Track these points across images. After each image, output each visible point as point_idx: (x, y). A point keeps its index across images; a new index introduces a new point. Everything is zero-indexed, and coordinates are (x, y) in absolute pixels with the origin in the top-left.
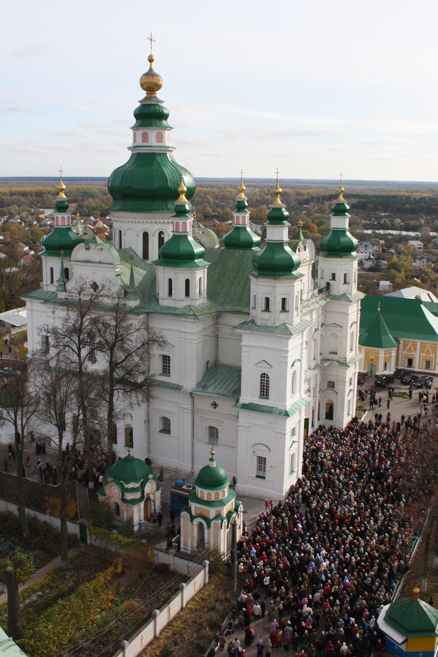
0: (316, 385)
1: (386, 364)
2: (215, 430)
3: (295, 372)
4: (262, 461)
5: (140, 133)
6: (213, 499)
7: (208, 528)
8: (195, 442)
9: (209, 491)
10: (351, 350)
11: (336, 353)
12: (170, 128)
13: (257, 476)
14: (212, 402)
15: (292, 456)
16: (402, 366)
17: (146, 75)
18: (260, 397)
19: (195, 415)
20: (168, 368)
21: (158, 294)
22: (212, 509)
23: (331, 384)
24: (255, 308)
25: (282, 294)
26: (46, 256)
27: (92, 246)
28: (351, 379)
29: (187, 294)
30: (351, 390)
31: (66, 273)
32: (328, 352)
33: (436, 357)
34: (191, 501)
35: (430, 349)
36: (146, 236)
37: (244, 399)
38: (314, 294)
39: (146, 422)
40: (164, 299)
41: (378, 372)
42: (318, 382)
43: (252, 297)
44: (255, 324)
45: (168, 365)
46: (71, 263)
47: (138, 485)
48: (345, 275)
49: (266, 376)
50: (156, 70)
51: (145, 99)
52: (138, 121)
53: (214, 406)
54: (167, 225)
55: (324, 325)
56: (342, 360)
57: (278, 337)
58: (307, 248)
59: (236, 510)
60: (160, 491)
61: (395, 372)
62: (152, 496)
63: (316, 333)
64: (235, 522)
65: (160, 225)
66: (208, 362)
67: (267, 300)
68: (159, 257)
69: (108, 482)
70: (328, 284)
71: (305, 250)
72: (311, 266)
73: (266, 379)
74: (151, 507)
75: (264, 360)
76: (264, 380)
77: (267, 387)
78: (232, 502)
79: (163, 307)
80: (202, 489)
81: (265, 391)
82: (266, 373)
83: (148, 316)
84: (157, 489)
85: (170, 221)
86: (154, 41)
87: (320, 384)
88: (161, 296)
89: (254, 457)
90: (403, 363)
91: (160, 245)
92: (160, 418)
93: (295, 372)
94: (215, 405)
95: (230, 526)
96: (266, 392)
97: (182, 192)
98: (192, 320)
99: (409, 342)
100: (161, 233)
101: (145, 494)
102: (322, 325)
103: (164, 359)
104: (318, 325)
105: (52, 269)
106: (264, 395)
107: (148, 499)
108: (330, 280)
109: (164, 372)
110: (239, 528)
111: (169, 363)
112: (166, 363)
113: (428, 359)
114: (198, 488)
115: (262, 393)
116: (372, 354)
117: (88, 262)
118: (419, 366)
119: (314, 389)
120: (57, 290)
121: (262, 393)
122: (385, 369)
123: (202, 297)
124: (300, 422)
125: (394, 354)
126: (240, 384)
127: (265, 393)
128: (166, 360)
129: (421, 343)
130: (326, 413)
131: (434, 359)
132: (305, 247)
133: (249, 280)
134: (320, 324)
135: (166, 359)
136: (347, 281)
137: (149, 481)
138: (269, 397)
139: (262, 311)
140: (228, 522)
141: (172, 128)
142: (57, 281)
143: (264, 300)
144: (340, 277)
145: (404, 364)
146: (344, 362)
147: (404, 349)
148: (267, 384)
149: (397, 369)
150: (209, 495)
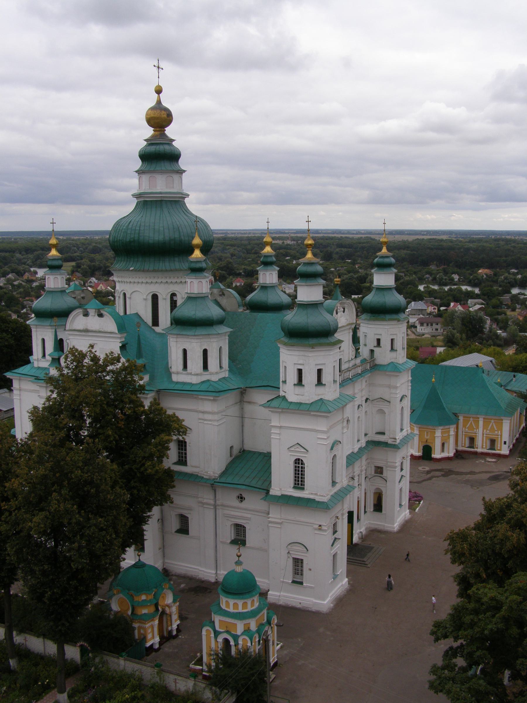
0: (361, 471)
1: (443, 445)
2: (242, 528)
3: (335, 456)
4: (298, 563)
5: (145, 177)
6: (240, 610)
7: (235, 645)
8: (218, 542)
9: (236, 601)
10: (402, 430)
11: (383, 433)
12: (181, 172)
13: (294, 582)
14: (238, 494)
16: (462, 446)
17: (152, 109)
18: (294, 488)
19: (217, 510)
20: (184, 455)
21: (171, 367)
22: (239, 622)
23: (379, 470)
24: (285, 382)
25: (316, 365)
26: (36, 325)
27: (92, 312)
28: (402, 463)
29: (205, 367)
30: (402, 476)
31: (59, 344)
32: (374, 433)
33: (501, 435)
34: (214, 614)
35: (494, 425)
36: (155, 298)
37: (275, 491)
38: (356, 365)
39: (160, 521)
40: (178, 373)
41: (434, 454)
42: (364, 468)
43: (282, 370)
44: (287, 400)
45: (184, 452)
46: (67, 333)
47: (151, 597)
48: (392, 340)
49: (300, 462)
50: (165, 104)
51: (153, 137)
52: (144, 163)
53: (240, 499)
54: (181, 285)
55: (368, 400)
56: (390, 441)
57: (314, 415)
58: (346, 309)
59: (269, 622)
60: (178, 604)
61: (455, 454)
62: (167, 609)
63: (360, 409)
64: (267, 637)
66: (232, 448)
67: (300, 371)
68: (172, 324)
69: (114, 595)
70: (372, 351)
71: (344, 312)
72: (351, 331)
73: (300, 465)
74: (167, 622)
75: (298, 443)
76: (299, 467)
77: (302, 474)
78: (264, 613)
79: (177, 383)
80: (227, 599)
81: (300, 479)
82: (300, 458)
83: (159, 394)
84: (174, 601)
85: (183, 281)
86: (162, 69)
87: (366, 470)
88: (174, 369)
89: (289, 559)
90: (463, 443)
91: (172, 310)
92: (176, 515)
93: (335, 456)
94: (242, 498)
95: (261, 642)
96: (302, 481)
97: (197, 246)
98: (212, 398)
99: (470, 418)
100: (173, 295)
101: (160, 609)
102: (367, 400)
103: (179, 445)
104: (362, 401)
105: (43, 340)
106: (298, 484)
107: (163, 613)
108: (374, 347)
109: (179, 460)
110: (273, 644)
111: (186, 450)
112: (182, 450)
113: (494, 437)
114: (223, 597)
115: (297, 482)
116: (427, 433)
117: (86, 331)
118: (483, 446)
119: (359, 476)
120: (49, 365)
121: (297, 482)
122: (443, 450)
123: (223, 370)
124: (343, 515)
125: (452, 432)
126: (271, 473)
127: (300, 482)
128: (182, 446)
129: (484, 419)
130: (375, 505)
131: (499, 436)
132: (344, 309)
133: (279, 348)
134: (364, 399)
135: (182, 445)
136: (395, 347)
137: (164, 590)
138: (305, 487)
139: (295, 385)
140: (259, 637)
141: (185, 171)
142: (49, 355)
144: (386, 343)
145: (465, 444)
146: (394, 443)
147: (464, 426)
148: (302, 471)
149: (457, 451)
150: (236, 605)
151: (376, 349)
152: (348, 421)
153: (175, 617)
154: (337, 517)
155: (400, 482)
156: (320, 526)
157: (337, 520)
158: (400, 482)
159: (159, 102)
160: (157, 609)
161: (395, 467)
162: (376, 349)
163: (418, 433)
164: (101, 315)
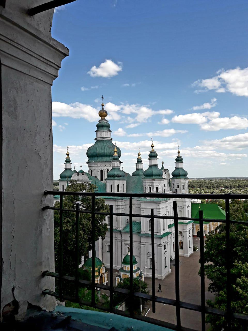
15: (165, 258)
25: (156, 185)
29: (118, 191)
34: (120, 271)
36: (102, 171)
48: (183, 185)
62: (103, 275)
65: (107, 167)
67: (150, 188)
71: (165, 173)
84: (106, 272)
91: (107, 173)
92: (107, 245)
100: (108, 170)
101: (100, 274)
107: (102, 276)
125: (208, 226)
143: (149, 189)
151: (178, 189)
152: (168, 212)
153: (106, 279)
154: (166, 243)
155: (189, 238)
156: (159, 245)
157: (166, 244)
158: (189, 238)
159: (103, 109)
160: (99, 274)
161: (187, 232)
162: (178, 189)
163: (195, 227)
164: (83, 175)
